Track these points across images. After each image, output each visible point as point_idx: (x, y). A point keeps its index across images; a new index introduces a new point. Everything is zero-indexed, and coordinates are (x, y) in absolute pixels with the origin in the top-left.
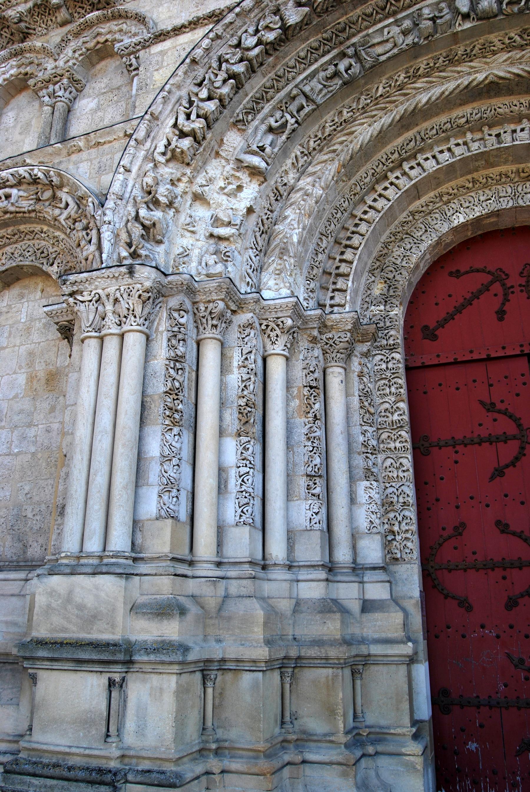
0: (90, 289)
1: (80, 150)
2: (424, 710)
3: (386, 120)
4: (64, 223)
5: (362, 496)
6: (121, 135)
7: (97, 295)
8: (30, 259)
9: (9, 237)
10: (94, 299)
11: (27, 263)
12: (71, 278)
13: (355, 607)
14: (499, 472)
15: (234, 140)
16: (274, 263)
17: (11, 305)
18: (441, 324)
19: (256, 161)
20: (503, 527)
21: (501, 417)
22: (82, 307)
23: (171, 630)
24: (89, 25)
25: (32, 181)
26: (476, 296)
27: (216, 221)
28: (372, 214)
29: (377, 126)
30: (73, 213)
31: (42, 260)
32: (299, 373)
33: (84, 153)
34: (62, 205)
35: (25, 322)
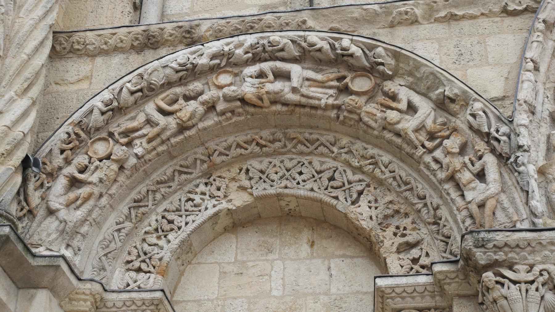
0: (531, 262)
1: (415, 22)
4: (412, 136)
6: (497, 9)
7: (545, 273)
8: (309, 185)
9: (261, 141)
10: (541, 279)
11: (302, 192)
12: (498, 238)
17: (244, 262)
22: (513, 291)
25: (333, 57)
30: (429, 123)
31: (335, 193)
33: (421, 27)
34: (403, 106)
35: (282, 297)
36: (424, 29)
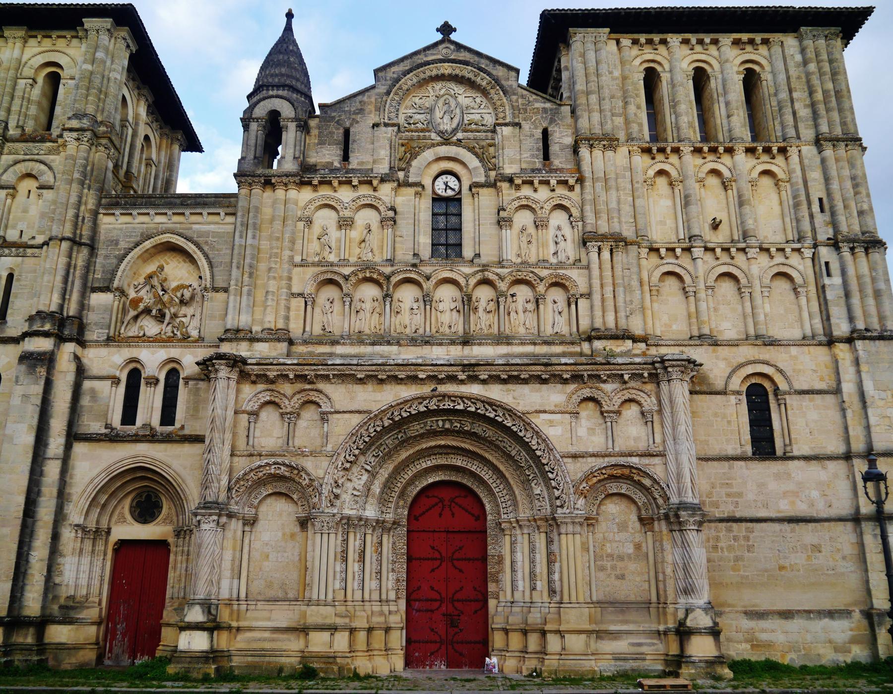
2: (404, 644)
3: (411, 451)
5: (390, 578)
13: (387, 613)
14: (433, 570)
15: (362, 459)
16: (370, 499)
18: (421, 515)
19: (369, 468)
20: (432, 588)
21: (436, 552)
23: (347, 620)
24: (305, 390)
26: (434, 506)
27: (355, 489)
28: (402, 480)
29: (408, 453)
32: (375, 538)
36: (310, 458)
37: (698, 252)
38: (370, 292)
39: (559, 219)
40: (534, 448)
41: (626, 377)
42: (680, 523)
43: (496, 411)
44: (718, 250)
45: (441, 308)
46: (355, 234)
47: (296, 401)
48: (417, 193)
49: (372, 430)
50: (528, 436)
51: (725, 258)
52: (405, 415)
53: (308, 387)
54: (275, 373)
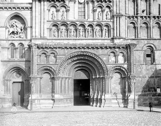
37: (139, 18)
38: (64, 28)
39: (107, 10)
40: (101, 63)
41: (121, 47)
42: (130, 78)
43: (92, 55)
44: (144, 17)
45: (80, 31)
46: (60, 13)
47: (50, 52)
48: (75, 3)
49: (66, 59)
50: (99, 60)
51: (145, 19)
52: (73, 56)
53: (52, 50)
54: (45, 47)
